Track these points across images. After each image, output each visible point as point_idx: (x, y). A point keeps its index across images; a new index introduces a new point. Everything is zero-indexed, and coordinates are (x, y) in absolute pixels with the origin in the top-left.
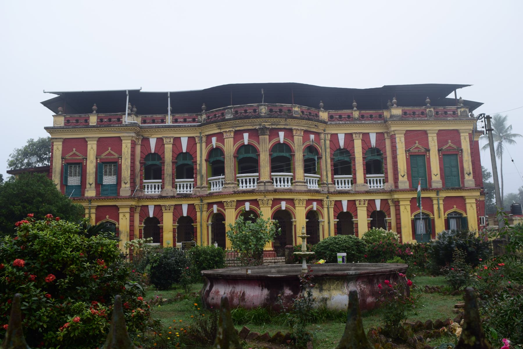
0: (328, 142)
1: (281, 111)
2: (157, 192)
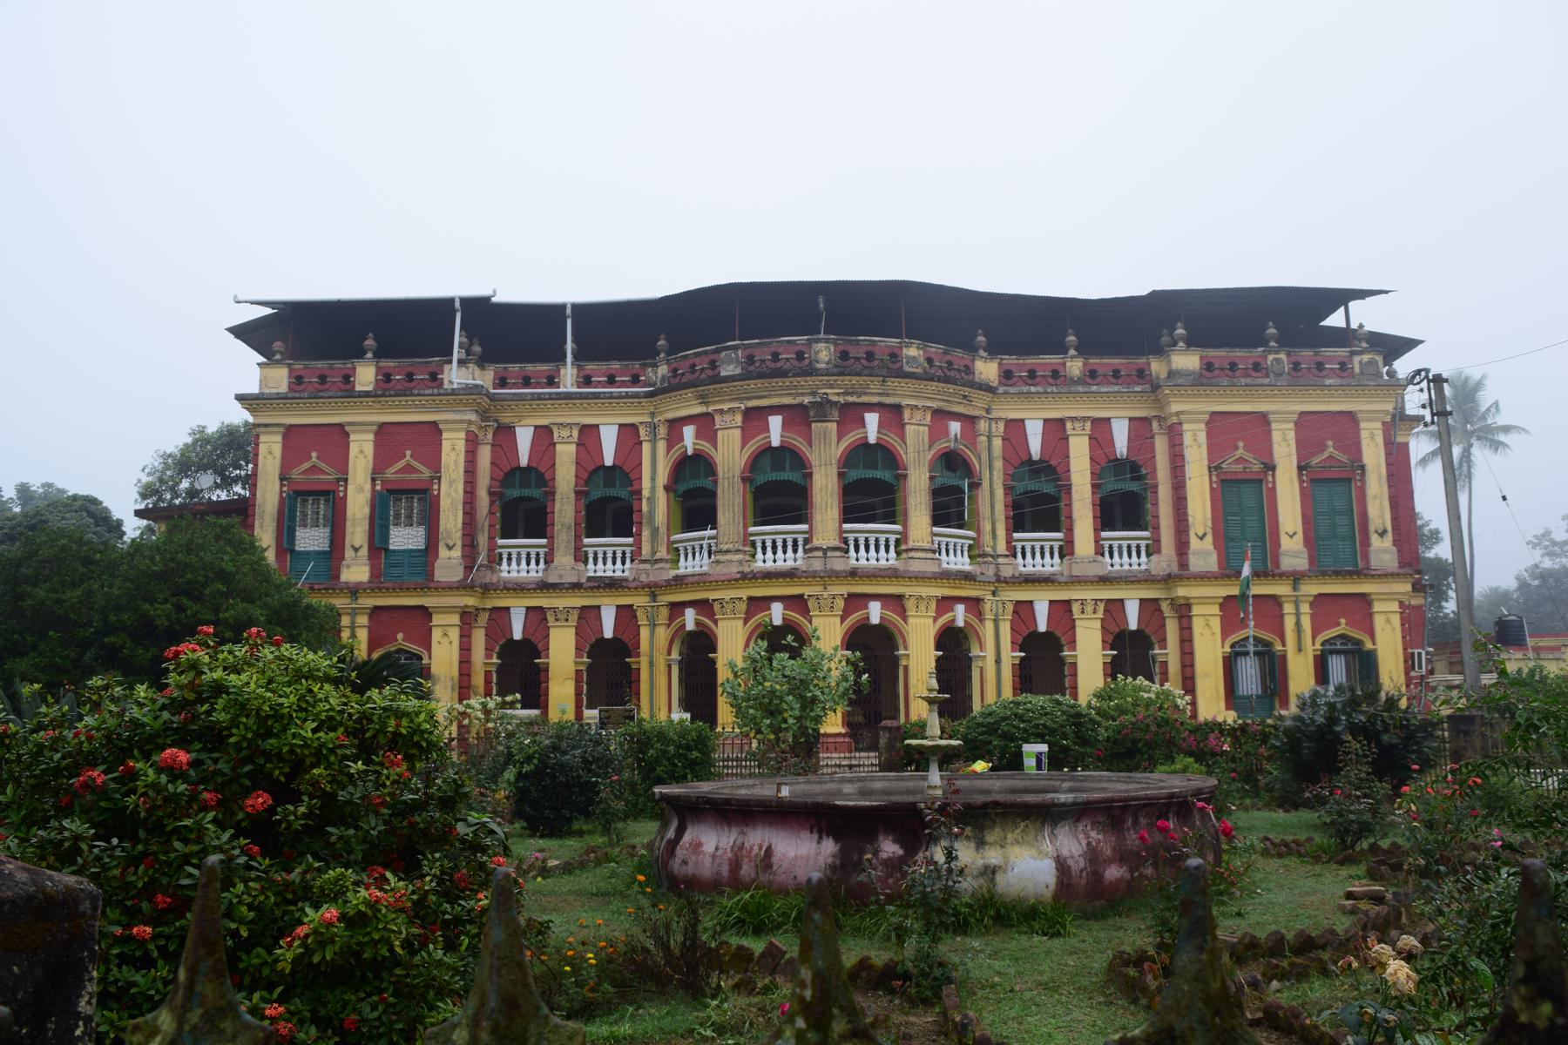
0: (997, 443)
1: (870, 356)
2: (534, 572)
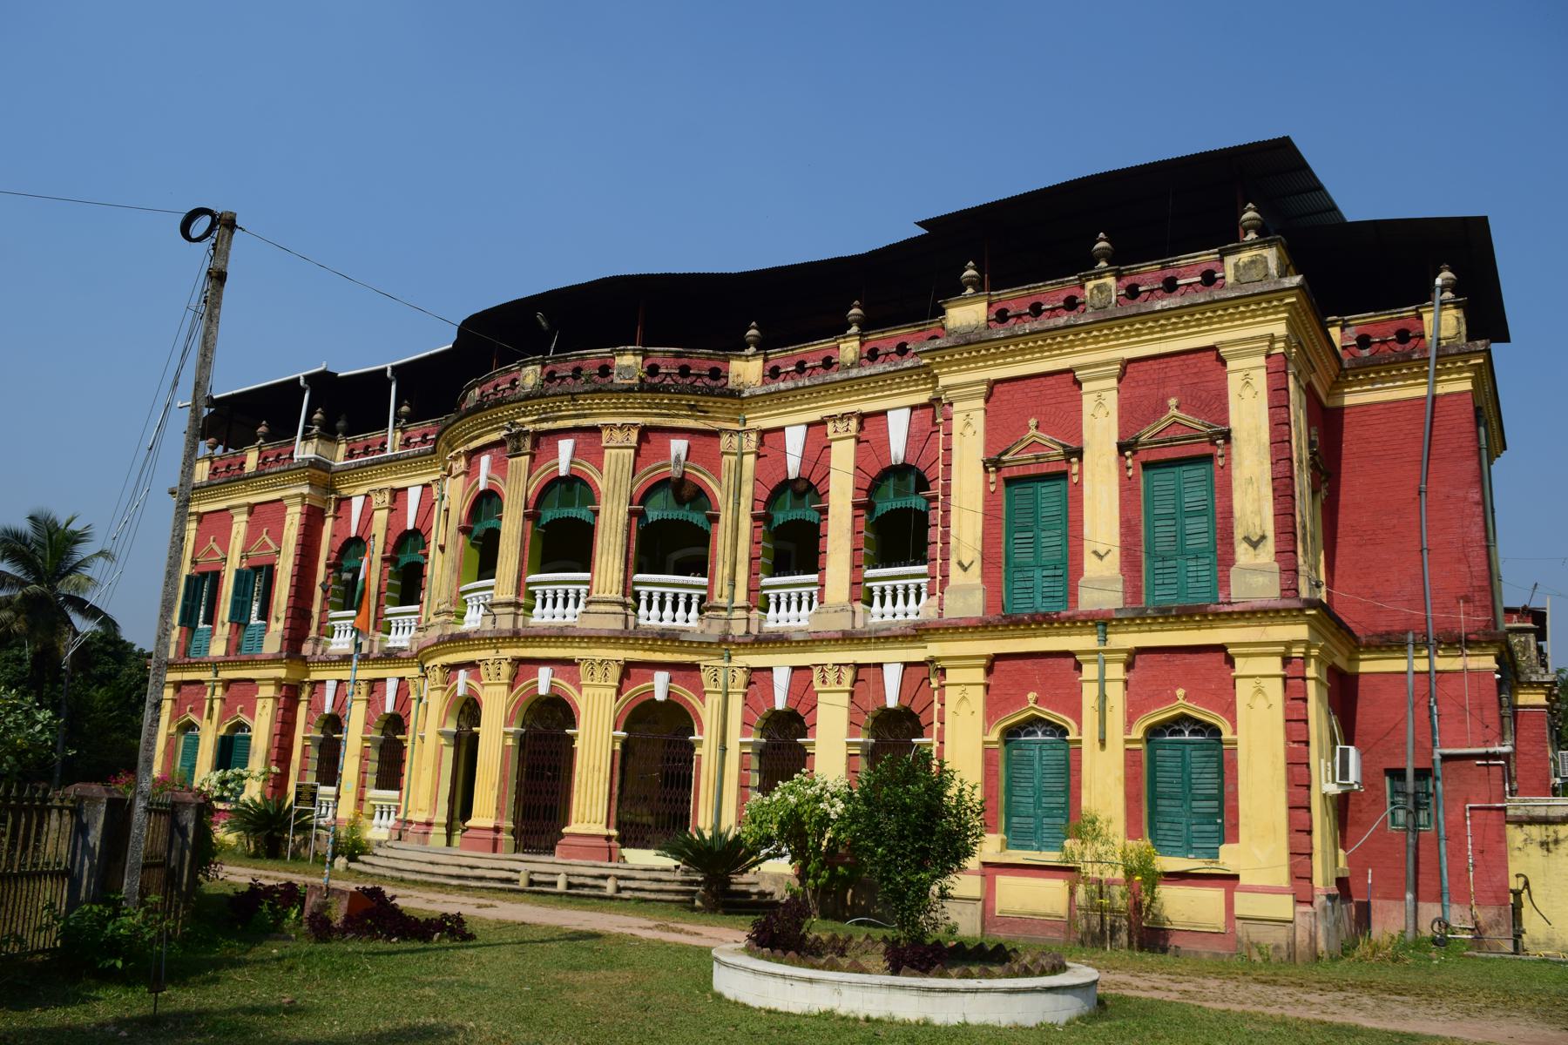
0: (749, 460)
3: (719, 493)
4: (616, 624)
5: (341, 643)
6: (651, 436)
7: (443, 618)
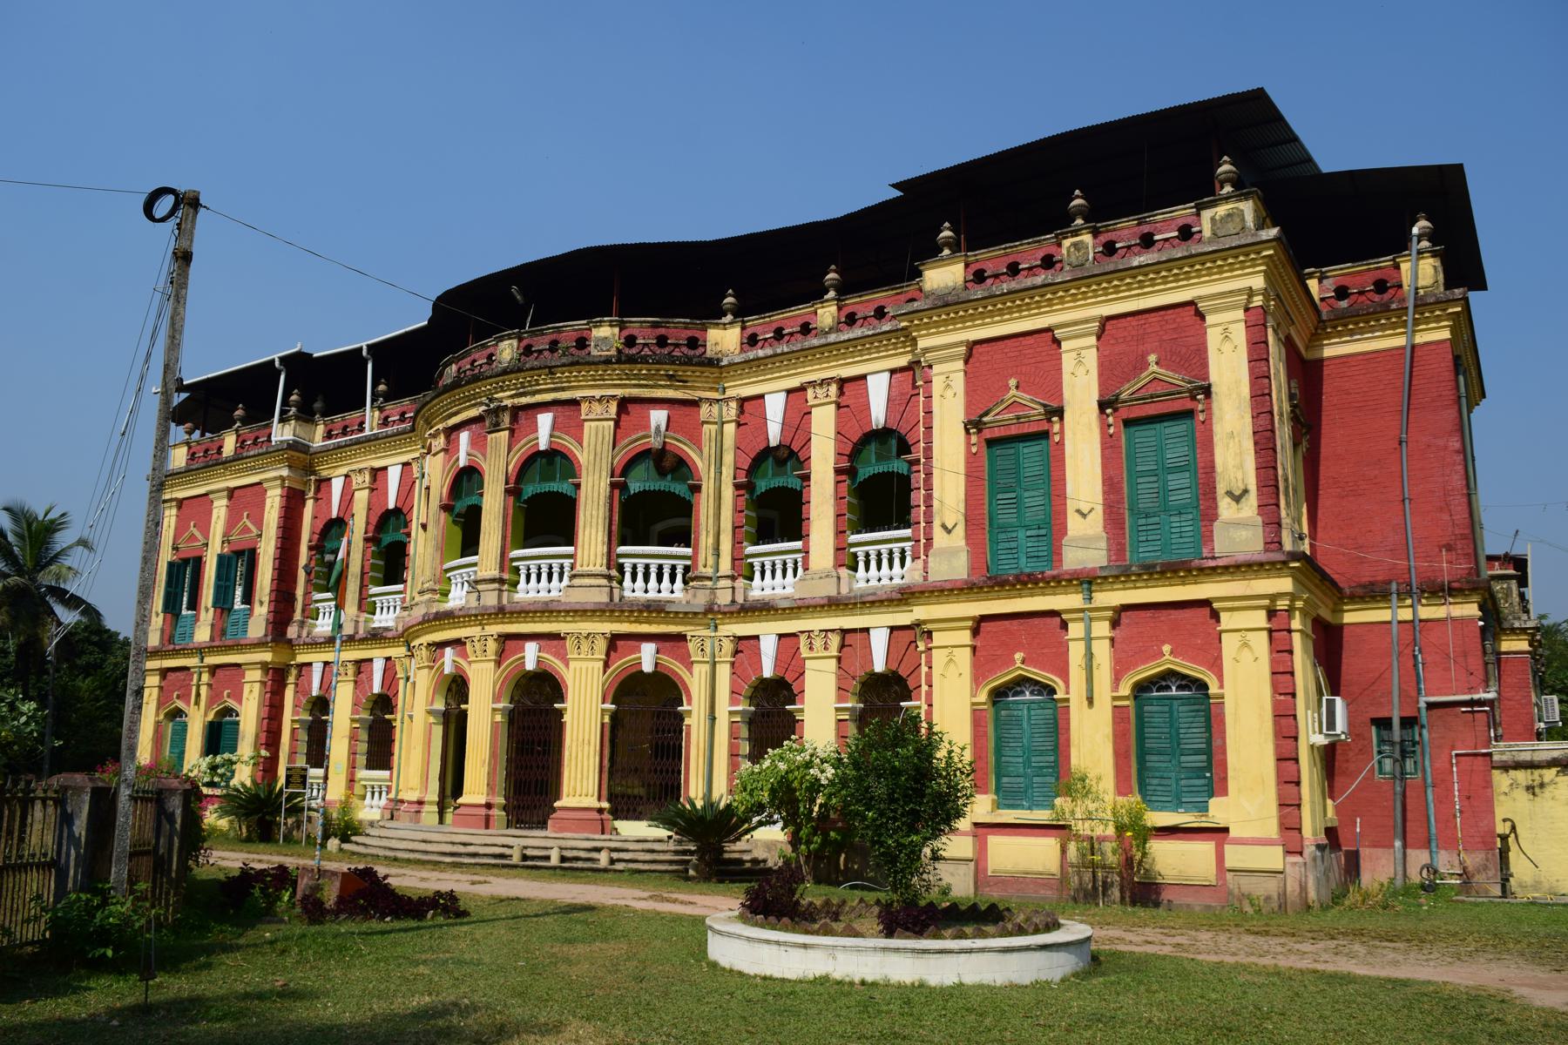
0: (730, 429)
3: (700, 462)
4: (602, 597)
5: (323, 626)
6: (631, 407)
7: (427, 596)
